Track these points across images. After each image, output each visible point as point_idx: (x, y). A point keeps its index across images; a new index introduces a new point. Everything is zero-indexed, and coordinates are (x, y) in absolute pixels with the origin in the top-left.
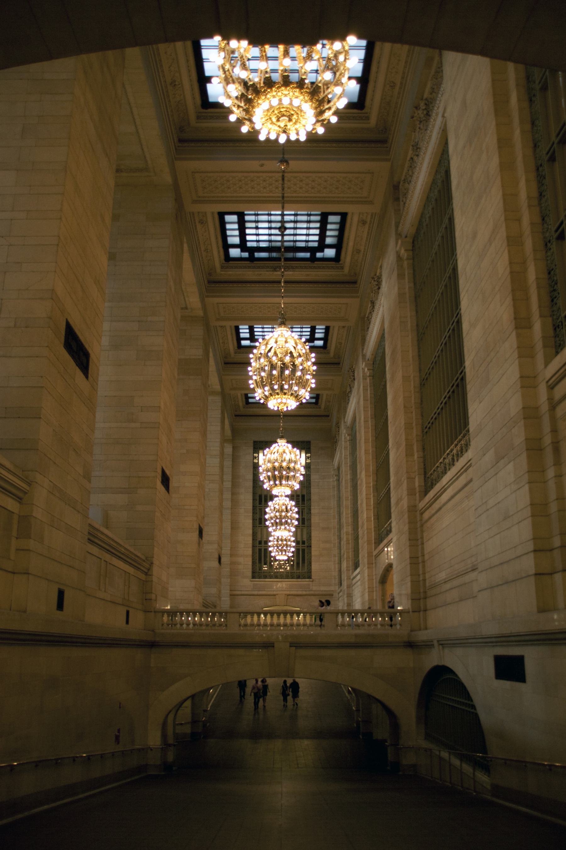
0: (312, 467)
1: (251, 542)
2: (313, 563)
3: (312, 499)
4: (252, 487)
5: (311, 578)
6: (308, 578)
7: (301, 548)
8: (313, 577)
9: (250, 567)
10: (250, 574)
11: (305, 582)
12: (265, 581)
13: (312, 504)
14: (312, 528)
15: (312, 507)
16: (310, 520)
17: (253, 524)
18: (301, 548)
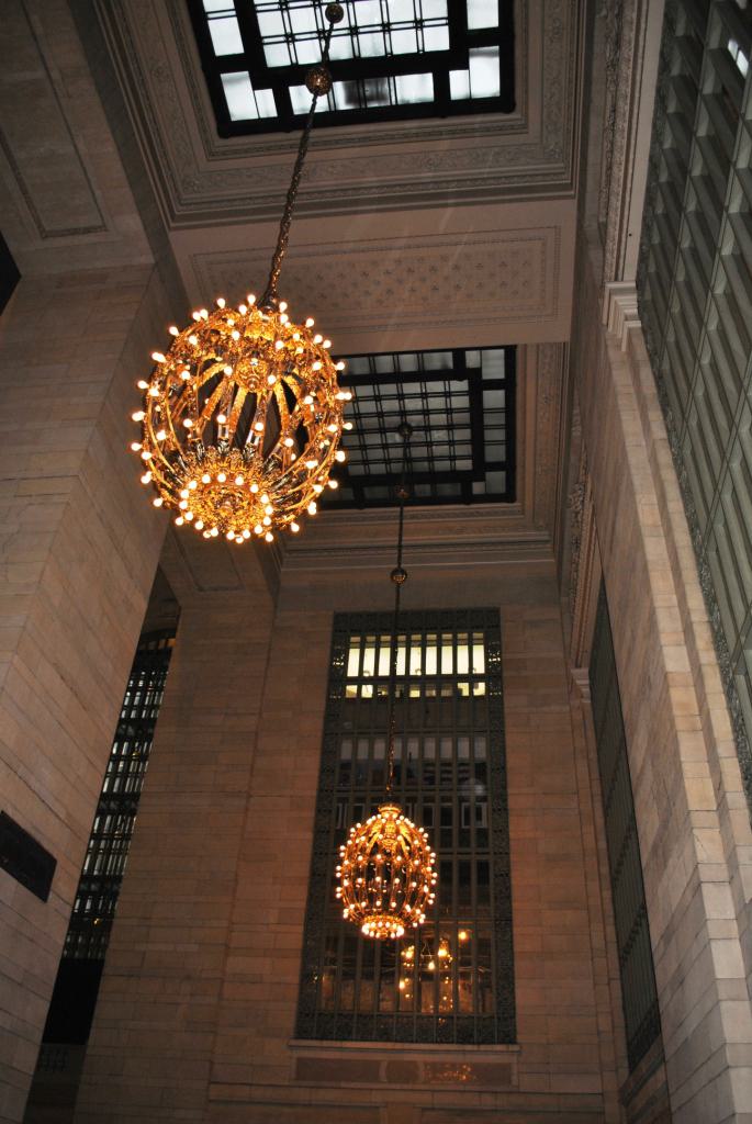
0: (505, 674)
1: (303, 904)
2: (518, 983)
3: (509, 766)
4: (320, 734)
5: (513, 1041)
6: (502, 1042)
7: (455, 859)
8: (519, 1038)
9: (294, 993)
10: (288, 1020)
11: (493, 1054)
12: (341, 1049)
13: (509, 778)
14: (513, 858)
15: (510, 791)
16: (503, 831)
17: (315, 847)
18: (455, 859)
